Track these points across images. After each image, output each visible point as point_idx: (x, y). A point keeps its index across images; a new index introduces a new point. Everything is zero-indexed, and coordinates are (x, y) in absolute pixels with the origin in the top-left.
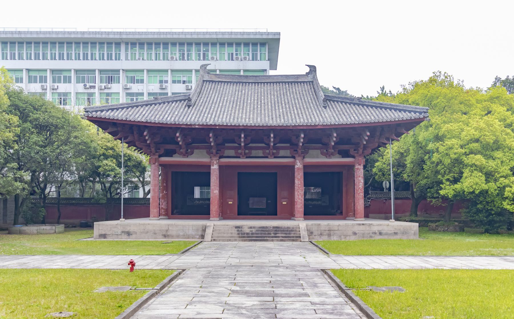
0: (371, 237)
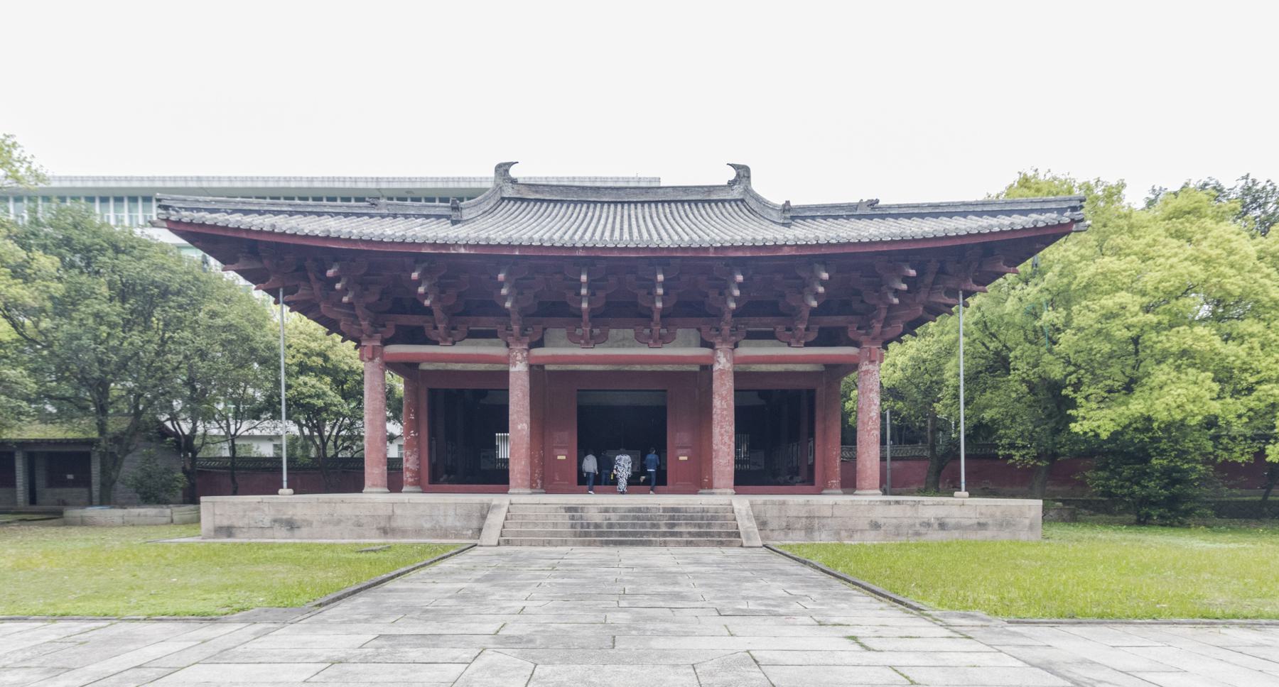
0: (917, 534)
